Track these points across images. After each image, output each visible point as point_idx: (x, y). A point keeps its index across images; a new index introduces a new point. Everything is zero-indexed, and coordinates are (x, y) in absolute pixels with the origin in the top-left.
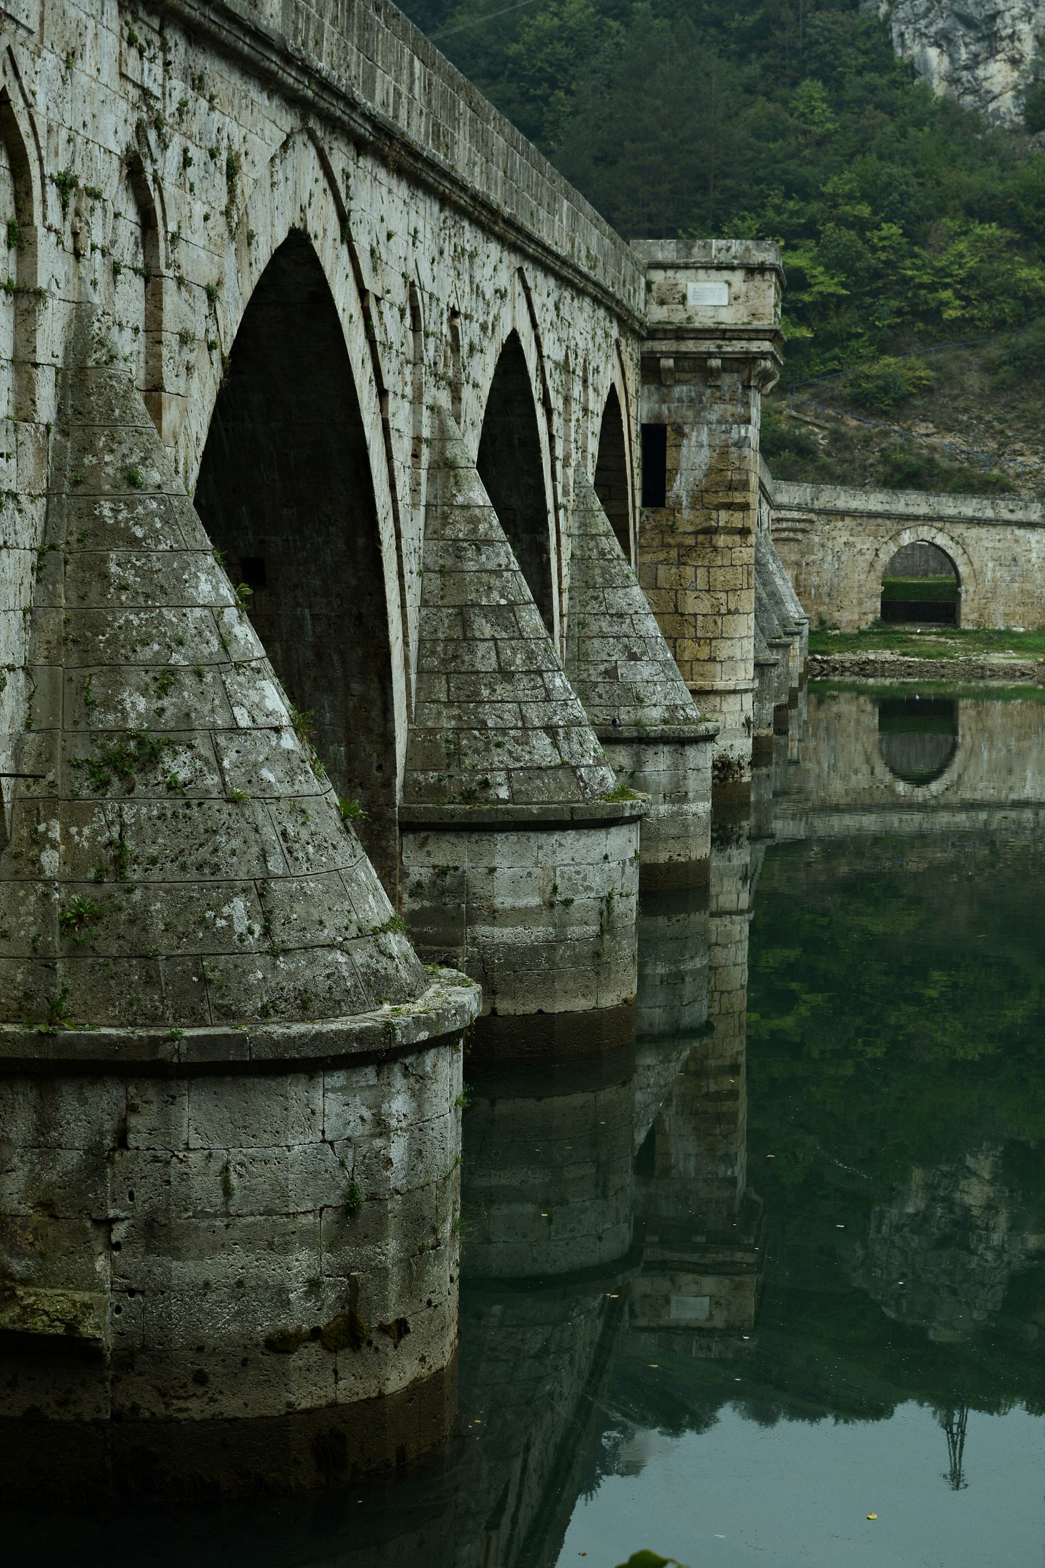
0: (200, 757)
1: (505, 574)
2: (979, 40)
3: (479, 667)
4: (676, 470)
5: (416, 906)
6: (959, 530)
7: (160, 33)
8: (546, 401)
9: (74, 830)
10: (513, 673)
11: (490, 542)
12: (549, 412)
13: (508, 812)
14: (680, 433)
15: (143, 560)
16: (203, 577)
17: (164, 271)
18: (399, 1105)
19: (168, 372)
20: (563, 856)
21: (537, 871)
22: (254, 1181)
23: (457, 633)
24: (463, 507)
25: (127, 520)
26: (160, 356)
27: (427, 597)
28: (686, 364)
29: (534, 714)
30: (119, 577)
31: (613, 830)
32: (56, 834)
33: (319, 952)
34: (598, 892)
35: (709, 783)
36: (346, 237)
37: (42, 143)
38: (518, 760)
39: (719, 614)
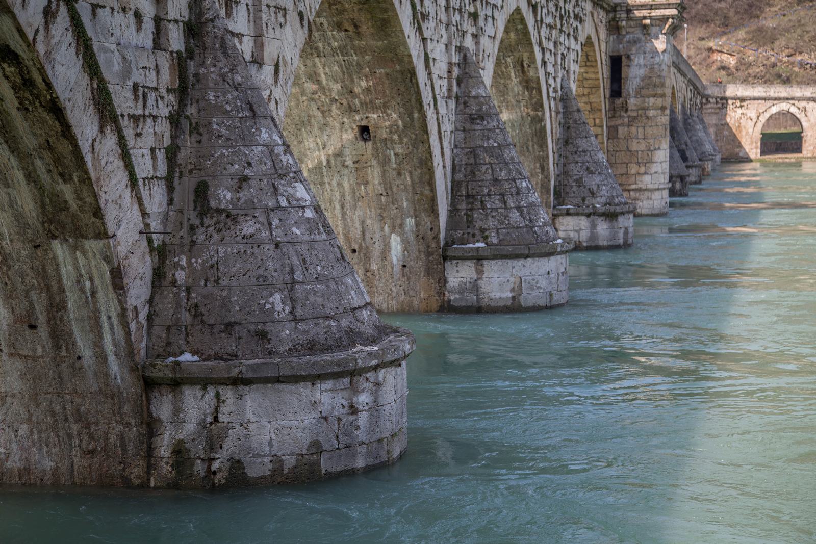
0: (259, 222)
1: (497, 131)
6: (803, 104)
8: (540, 44)
10: (500, 181)
12: (543, 49)
14: (628, 57)
15: (231, 122)
16: (263, 131)
18: (363, 399)
21: (512, 280)
22: (285, 438)
23: (472, 161)
24: (476, 97)
26: (261, 18)
27: (457, 143)
28: (632, 23)
31: (552, 258)
32: (184, 262)
34: (544, 289)
39: (649, 150)
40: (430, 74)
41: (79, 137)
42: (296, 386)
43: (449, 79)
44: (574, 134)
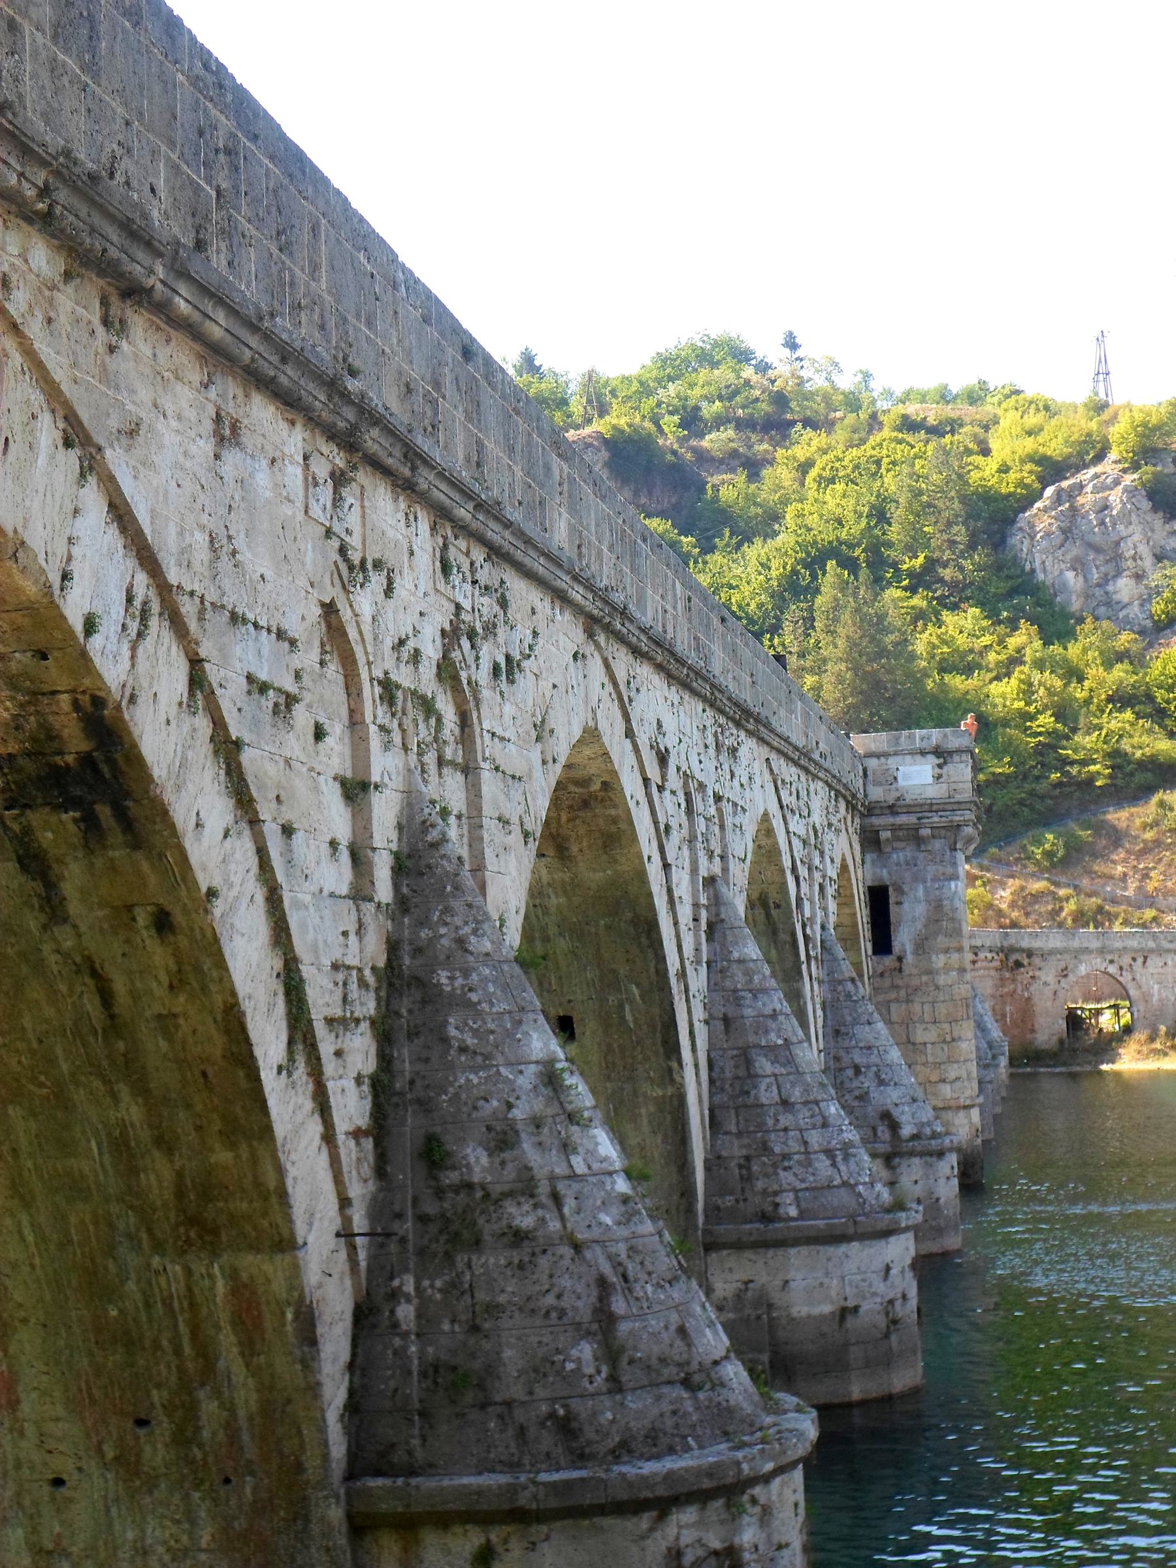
2: (1107, 562)
3: (764, 1100)
4: (899, 923)
7: (467, 554)
8: (794, 869)
9: (426, 1283)
10: (793, 1105)
11: (765, 991)
13: (798, 1228)
14: (900, 890)
16: (535, 1036)
17: (483, 765)
19: (489, 853)
20: (851, 1266)
23: (742, 1072)
24: (740, 961)
25: (463, 986)
29: (815, 1138)
31: (892, 1239)
32: (409, 1287)
33: (665, 1390)
35: (957, 1189)
36: (629, 734)
37: (370, 649)
38: (803, 1181)
39: (944, 1041)
40: (676, 923)
41: (261, 1063)
42: (635, 1520)
43: (697, 930)
44: (849, 1019)
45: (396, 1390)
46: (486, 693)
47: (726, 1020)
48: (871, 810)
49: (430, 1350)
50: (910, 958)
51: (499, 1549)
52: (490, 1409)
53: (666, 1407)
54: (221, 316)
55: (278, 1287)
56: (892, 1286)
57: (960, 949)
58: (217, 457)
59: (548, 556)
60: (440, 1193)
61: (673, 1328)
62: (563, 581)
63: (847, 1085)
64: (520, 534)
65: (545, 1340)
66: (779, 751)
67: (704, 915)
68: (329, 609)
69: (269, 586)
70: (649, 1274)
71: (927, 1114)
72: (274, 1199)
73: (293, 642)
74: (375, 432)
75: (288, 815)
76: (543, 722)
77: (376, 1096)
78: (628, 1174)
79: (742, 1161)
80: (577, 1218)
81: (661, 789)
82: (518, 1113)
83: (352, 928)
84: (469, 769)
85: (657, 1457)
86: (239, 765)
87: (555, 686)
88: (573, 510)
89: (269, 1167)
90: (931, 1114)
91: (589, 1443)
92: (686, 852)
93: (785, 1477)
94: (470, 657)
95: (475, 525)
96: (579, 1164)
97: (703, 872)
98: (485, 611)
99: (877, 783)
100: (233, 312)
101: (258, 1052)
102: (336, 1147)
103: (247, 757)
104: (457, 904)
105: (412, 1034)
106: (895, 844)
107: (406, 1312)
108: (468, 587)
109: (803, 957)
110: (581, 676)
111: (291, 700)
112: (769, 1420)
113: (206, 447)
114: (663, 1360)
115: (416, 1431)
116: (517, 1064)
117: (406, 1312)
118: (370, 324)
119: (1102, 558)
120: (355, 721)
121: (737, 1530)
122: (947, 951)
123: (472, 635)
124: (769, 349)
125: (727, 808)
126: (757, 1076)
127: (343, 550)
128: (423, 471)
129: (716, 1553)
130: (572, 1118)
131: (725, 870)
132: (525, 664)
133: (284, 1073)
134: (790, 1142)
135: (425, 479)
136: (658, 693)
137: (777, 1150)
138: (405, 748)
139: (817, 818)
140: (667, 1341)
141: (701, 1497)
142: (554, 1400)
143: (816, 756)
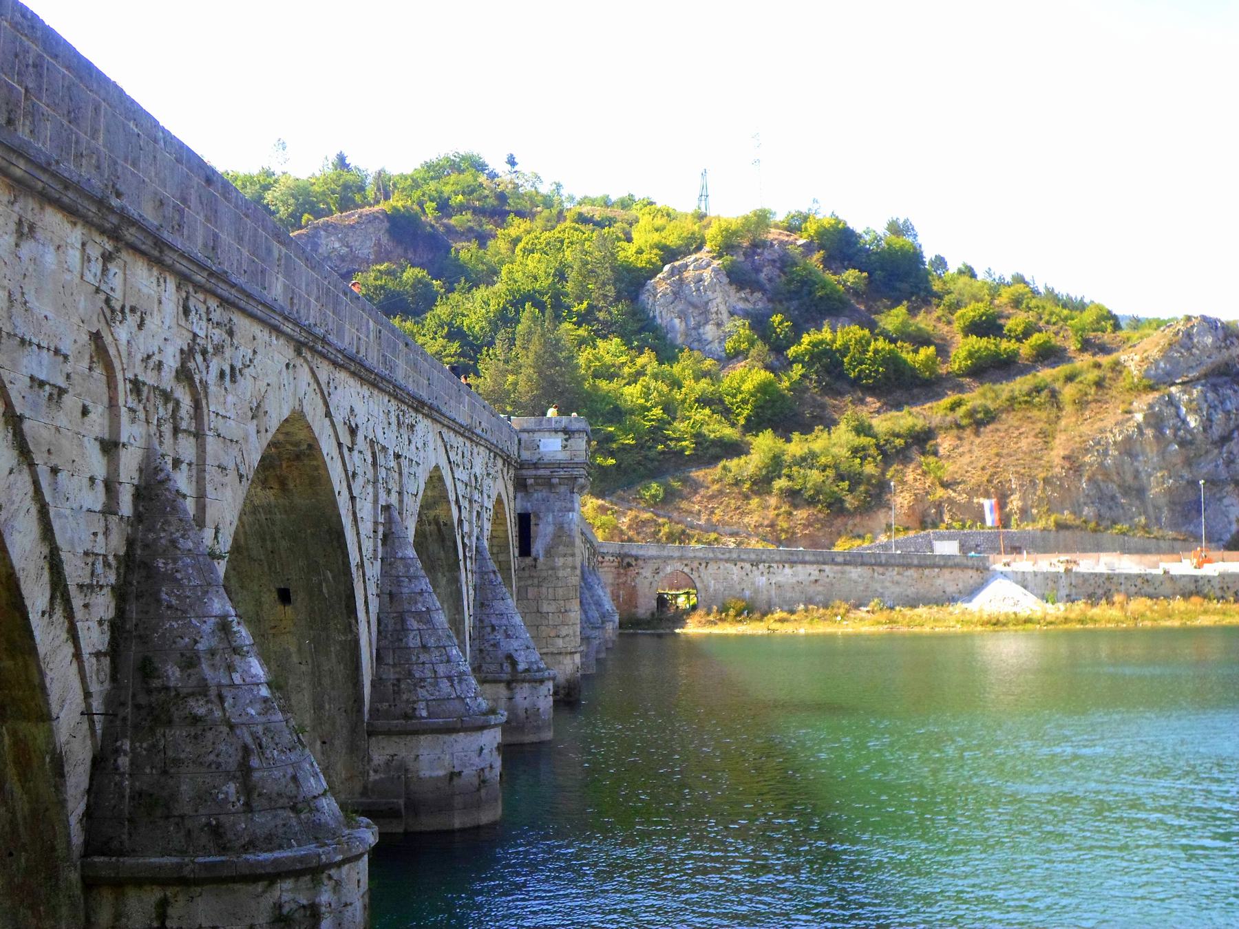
2: (701, 314)
3: (412, 645)
5: (377, 777)
7: (205, 302)
8: (457, 501)
9: (138, 744)
10: (429, 648)
11: (416, 577)
12: (460, 508)
13: (426, 723)
16: (216, 601)
17: (208, 433)
19: (209, 488)
20: (458, 747)
23: (399, 627)
24: (401, 558)
25: (172, 569)
29: (442, 669)
30: (166, 601)
31: (485, 732)
32: (127, 745)
33: (279, 812)
35: (552, 704)
36: (328, 414)
37: (124, 361)
38: (432, 695)
39: (560, 612)
40: (358, 534)
41: (30, 609)
43: (375, 538)
44: (490, 596)
45: (115, 807)
46: (213, 389)
47: (391, 595)
48: (522, 465)
49: (137, 784)
50: (541, 559)
51: (172, 900)
52: (171, 820)
53: (280, 822)
54: (22, 163)
55: (41, 741)
56: (484, 760)
57: (573, 555)
58: (17, 245)
59: (264, 305)
60: (149, 692)
61: (288, 776)
62: (277, 320)
63: (486, 637)
64: (242, 291)
65: (207, 781)
66: (449, 427)
67: (381, 529)
68: (96, 337)
69: (51, 323)
70: (277, 744)
71: (535, 656)
72: (38, 690)
73: (66, 357)
74: (133, 230)
75: (54, 461)
76: (259, 406)
77: (113, 632)
78: (269, 685)
79: (395, 682)
80: (234, 710)
81: (351, 450)
82: (200, 646)
83: (101, 531)
84: (199, 435)
85: (271, 850)
86: (22, 430)
87: (268, 385)
88: (288, 275)
89: (35, 671)
90: (538, 656)
91: (230, 841)
92: (370, 489)
93: (352, 864)
94: (202, 367)
95: (208, 286)
96: (237, 678)
97: (382, 502)
98: (215, 338)
99: (527, 449)
100: (29, 161)
101: (28, 603)
102: (83, 661)
103: (27, 426)
104: (173, 519)
105: (139, 596)
106: (536, 488)
107: (124, 762)
108: (204, 323)
109: (461, 556)
110: (291, 378)
111: (62, 391)
112: (347, 832)
113: (10, 239)
114: (279, 795)
115: (126, 830)
116: (203, 617)
117: (124, 762)
118: (134, 164)
119: (697, 311)
120: (112, 405)
121: (318, 894)
122: (565, 556)
123: (204, 352)
124: (497, 164)
125: (405, 463)
126: (408, 630)
127: (108, 301)
128: (167, 252)
129: (304, 907)
130: (236, 650)
131: (401, 501)
132: (246, 371)
133: (47, 615)
134: (426, 671)
135: (169, 258)
136: (352, 390)
137: (417, 675)
138: (148, 422)
139: (478, 469)
140: (284, 784)
141: (296, 874)
142: (210, 816)
143: (478, 431)
